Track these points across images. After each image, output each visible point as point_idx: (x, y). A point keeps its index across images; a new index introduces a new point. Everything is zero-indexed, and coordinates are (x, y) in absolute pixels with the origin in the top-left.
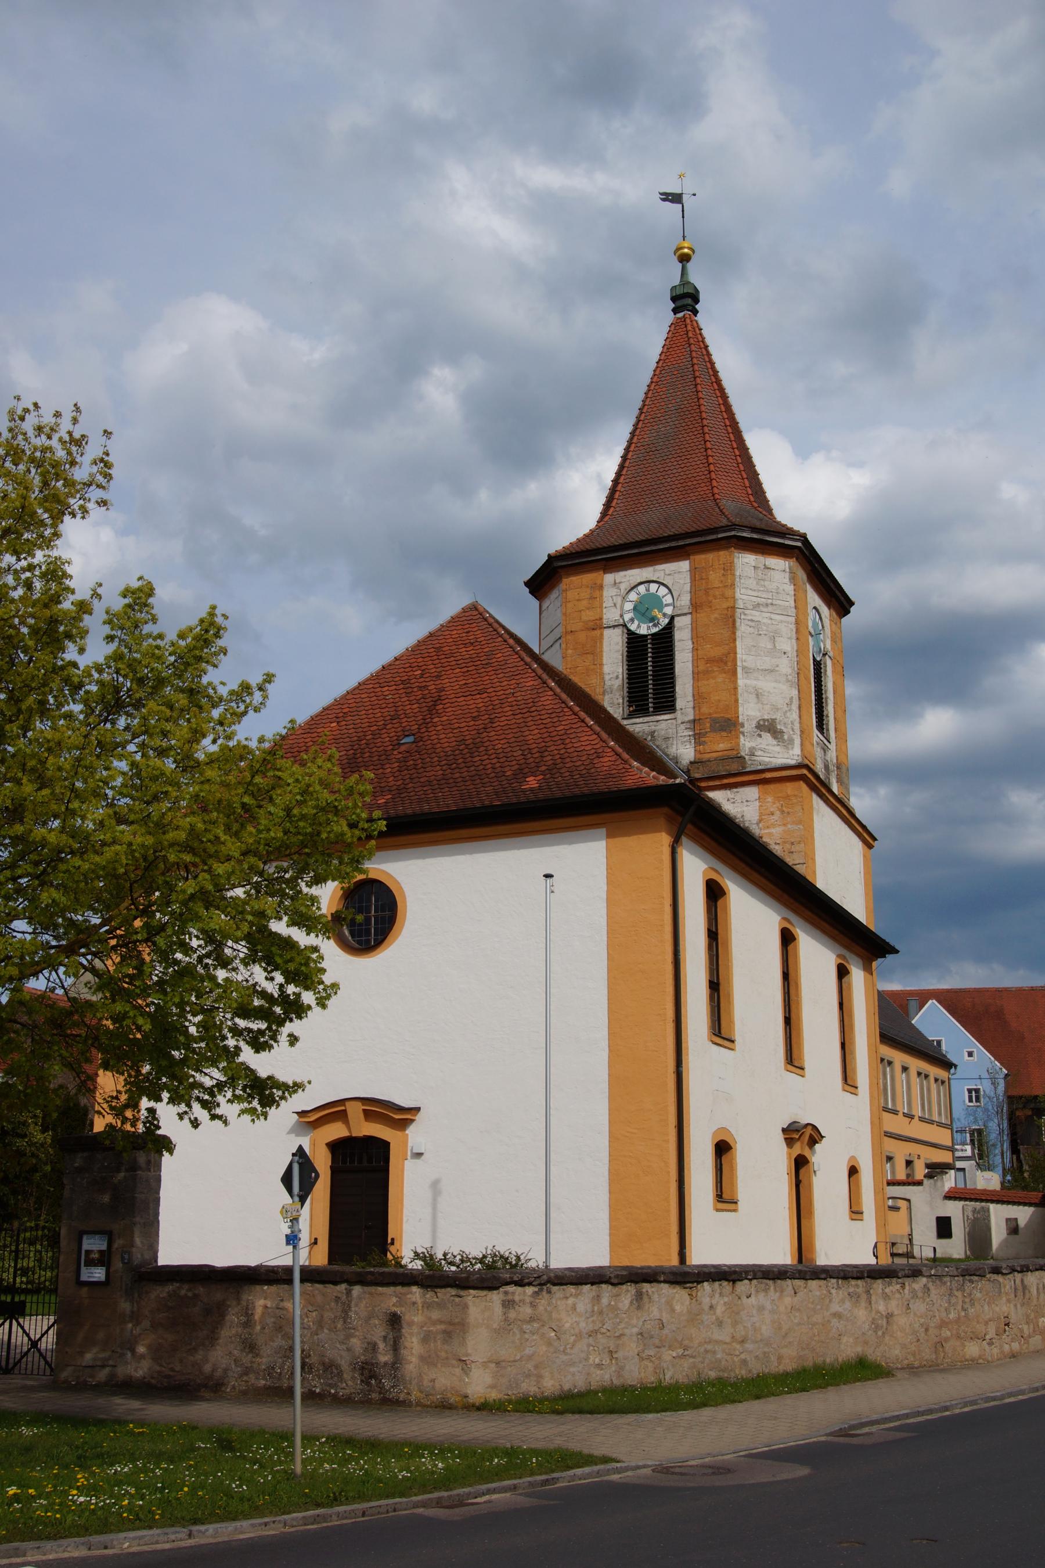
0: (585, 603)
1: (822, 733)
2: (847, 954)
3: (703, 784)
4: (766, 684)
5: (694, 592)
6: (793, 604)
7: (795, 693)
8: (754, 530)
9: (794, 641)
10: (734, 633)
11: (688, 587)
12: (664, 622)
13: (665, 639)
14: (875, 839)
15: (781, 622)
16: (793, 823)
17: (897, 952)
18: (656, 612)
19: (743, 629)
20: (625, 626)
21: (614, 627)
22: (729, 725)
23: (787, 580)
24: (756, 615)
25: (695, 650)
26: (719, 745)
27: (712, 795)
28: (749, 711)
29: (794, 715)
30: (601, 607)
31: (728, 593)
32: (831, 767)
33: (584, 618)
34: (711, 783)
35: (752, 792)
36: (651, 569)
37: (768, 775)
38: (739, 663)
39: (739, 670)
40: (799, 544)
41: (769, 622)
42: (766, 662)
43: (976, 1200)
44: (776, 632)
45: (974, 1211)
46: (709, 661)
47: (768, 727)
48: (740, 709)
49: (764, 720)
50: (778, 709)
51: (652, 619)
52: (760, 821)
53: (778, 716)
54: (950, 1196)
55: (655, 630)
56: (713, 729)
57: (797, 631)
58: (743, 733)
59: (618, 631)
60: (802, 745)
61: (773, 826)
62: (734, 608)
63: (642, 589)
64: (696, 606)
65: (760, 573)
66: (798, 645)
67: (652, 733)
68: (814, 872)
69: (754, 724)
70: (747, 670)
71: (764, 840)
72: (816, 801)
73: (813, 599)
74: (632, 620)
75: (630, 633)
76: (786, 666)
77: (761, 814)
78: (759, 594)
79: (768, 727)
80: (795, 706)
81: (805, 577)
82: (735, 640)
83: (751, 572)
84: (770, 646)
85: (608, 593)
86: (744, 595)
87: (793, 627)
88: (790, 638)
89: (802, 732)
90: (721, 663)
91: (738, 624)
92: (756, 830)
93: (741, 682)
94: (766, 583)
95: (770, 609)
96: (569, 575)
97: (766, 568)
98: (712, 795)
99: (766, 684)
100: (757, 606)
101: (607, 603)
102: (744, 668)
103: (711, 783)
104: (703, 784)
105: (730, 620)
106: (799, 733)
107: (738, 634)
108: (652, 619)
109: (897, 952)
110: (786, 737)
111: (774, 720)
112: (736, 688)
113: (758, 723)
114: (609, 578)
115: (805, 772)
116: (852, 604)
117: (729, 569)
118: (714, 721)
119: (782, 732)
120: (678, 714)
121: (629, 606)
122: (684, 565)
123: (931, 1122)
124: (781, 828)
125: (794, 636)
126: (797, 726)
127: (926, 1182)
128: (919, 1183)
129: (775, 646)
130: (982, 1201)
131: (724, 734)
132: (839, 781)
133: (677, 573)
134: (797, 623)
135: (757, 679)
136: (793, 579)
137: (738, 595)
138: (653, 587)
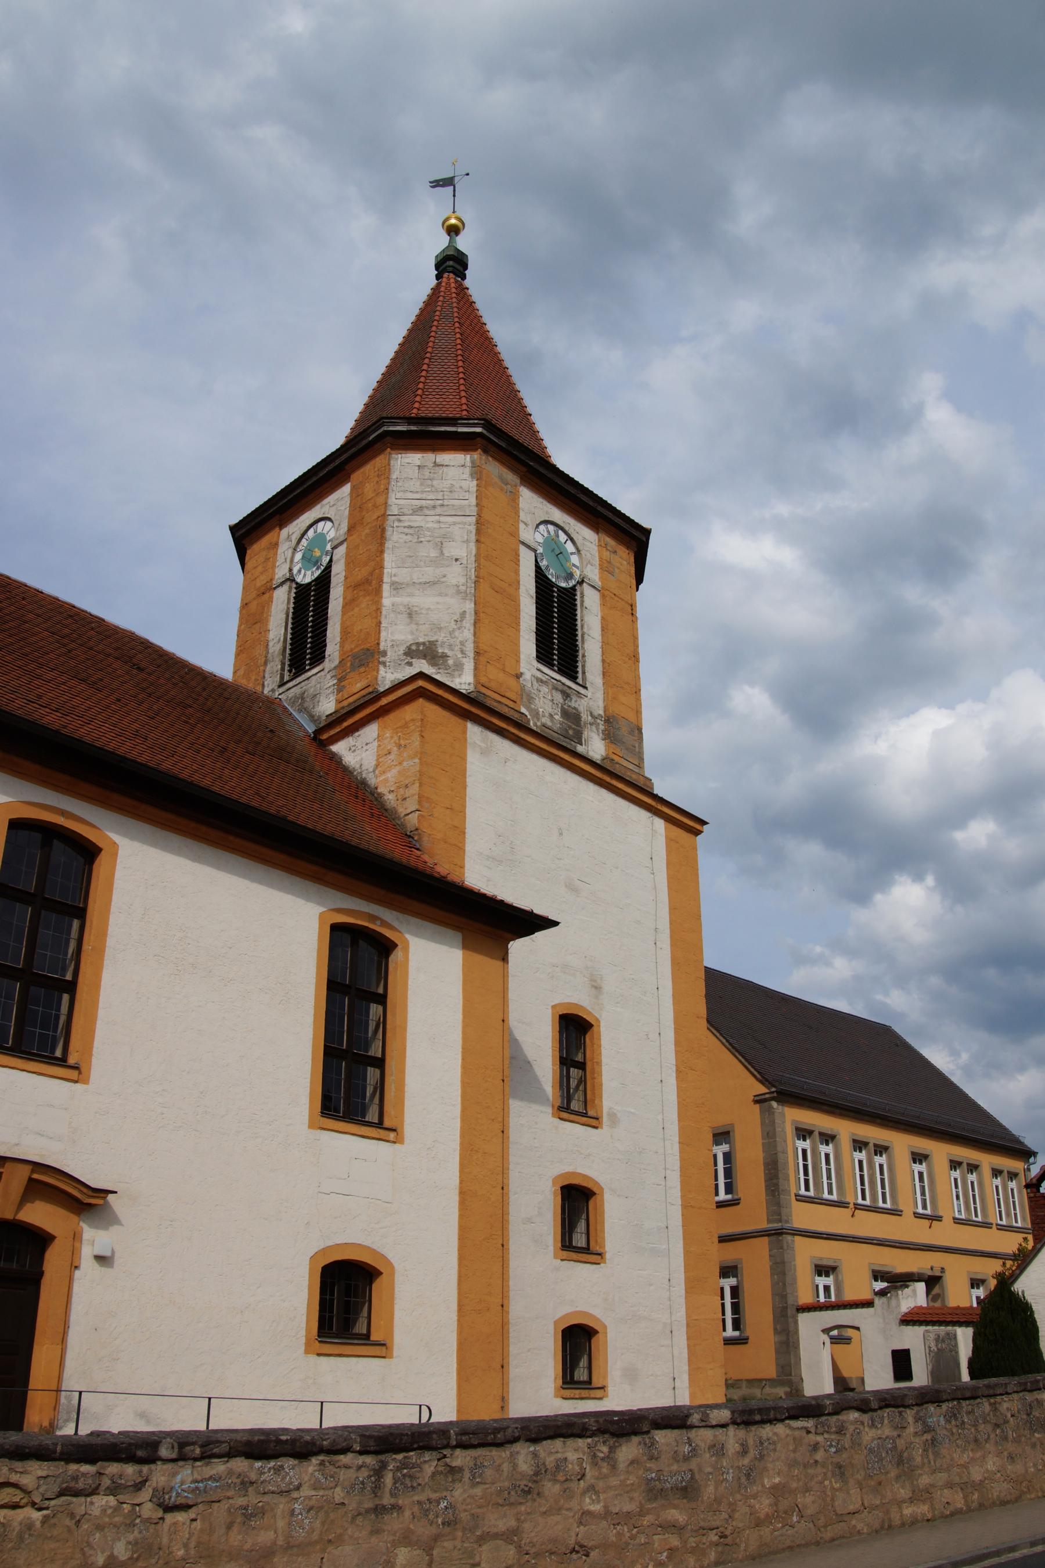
0: (260, 569)
1: (573, 678)
2: (388, 915)
3: (325, 736)
4: (423, 600)
5: (351, 515)
6: (473, 501)
7: (469, 606)
8: (410, 420)
9: (473, 546)
11: (347, 512)
12: (325, 560)
13: (323, 582)
14: (703, 823)
15: (455, 524)
16: (411, 758)
17: (555, 924)
18: (317, 553)
19: (395, 537)
20: (291, 579)
21: (282, 584)
22: (367, 655)
24: (417, 520)
25: (346, 578)
26: (357, 685)
27: (335, 748)
28: (395, 635)
29: (467, 633)
30: (274, 567)
31: (380, 500)
32: (585, 717)
33: (259, 584)
34: (332, 732)
35: (371, 731)
36: (318, 507)
37: (384, 701)
38: (386, 579)
39: (386, 587)
40: (479, 430)
41: (436, 525)
42: (430, 573)
43: (940, 1323)
44: (444, 536)
45: (938, 1339)
46: (357, 586)
48: (383, 634)
49: (418, 644)
50: (440, 629)
51: (317, 563)
52: (377, 766)
53: (440, 637)
54: (909, 1320)
55: (317, 573)
56: (353, 668)
57: (478, 532)
58: (384, 664)
59: (286, 587)
60: (476, 669)
61: (390, 768)
62: (384, 516)
63: (311, 533)
64: (351, 529)
65: (426, 472)
66: (478, 549)
67: (302, 697)
68: (460, 831)
69: (402, 649)
70: (396, 587)
71: (379, 790)
72: (474, 732)
73: (532, 504)
74: (299, 571)
75: (299, 586)
76: (458, 576)
77: (379, 757)
78: (424, 496)
79: (428, 651)
80: (468, 623)
81: (511, 477)
82: (382, 552)
83: (414, 473)
84: (434, 553)
85: (284, 549)
86: (397, 500)
87: (473, 528)
88: (467, 541)
89: (477, 653)
90: (368, 585)
91: (389, 531)
92: (372, 781)
93: (387, 601)
94: (435, 483)
95: (439, 511)
96: (252, 543)
97: (436, 464)
98: (335, 748)
99: (423, 600)
100: (418, 510)
101: (280, 558)
102: (393, 583)
103: (332, 732)
104: (325, 736)
105: (380, 536)
106: (472, 655)
107: (388, 545)
108: (317, 563)
109: (555, 924)
110: (450, 662)
111: (433, 644)
112: (378, 610)
113: (409, 648)
114: (284, 532)
115: (421, 683)
116: (647, 532)
117: (385, 474)
118: (355, 657)
119: (445, 656)
120: (328, 664)
121: (298, 556)
122: (346, 489)
123: (986, 1225)
124: (398, 768)
125: (473, 537)
126: (470, 648)
127: (877, 1301)
128: (869, 1304)
129: (442, 553)
130: (947, 1323)
131: (362, 669)
132: (610, 736)
133: (338, 502)
134: (480, 524)
135: (411, 595)
136: (477, 473)
137: (392, 500)
138: (321, 524)
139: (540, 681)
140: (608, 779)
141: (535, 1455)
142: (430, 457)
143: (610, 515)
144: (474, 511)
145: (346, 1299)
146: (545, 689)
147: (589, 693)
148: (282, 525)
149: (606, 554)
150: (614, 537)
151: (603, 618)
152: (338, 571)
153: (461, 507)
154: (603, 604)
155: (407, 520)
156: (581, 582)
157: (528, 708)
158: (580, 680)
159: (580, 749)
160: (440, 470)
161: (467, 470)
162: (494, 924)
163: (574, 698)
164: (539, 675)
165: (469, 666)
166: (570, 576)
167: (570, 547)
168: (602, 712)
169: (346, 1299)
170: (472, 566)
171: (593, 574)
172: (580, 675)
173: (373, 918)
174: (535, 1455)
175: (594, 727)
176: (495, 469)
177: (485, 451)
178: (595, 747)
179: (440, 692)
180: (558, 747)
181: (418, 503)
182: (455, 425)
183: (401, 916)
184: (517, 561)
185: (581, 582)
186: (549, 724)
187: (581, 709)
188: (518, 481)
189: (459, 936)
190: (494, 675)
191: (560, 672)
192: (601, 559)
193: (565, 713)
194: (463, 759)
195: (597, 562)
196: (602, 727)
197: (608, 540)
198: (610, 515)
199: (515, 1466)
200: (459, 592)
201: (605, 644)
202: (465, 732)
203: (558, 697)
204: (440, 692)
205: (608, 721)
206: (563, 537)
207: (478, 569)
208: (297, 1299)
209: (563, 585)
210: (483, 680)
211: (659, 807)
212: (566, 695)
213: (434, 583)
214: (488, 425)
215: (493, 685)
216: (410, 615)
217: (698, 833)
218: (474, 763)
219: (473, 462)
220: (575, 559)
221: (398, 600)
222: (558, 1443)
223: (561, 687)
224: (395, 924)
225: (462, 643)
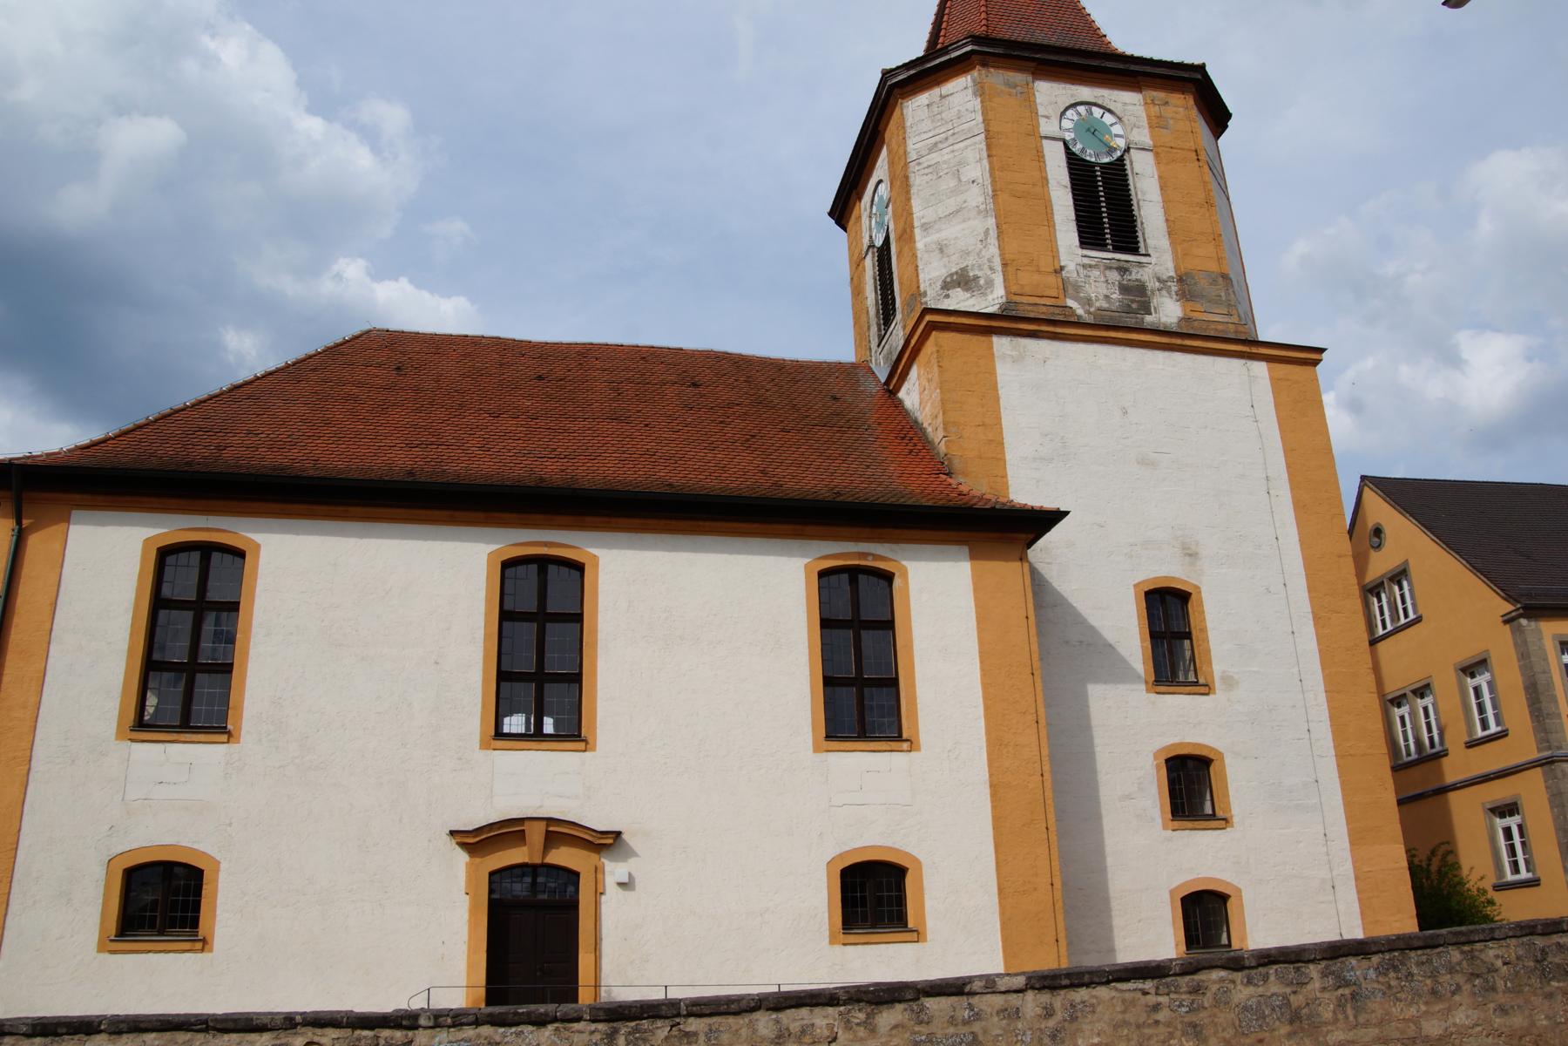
4: (950, 232)
7: (991, 222)
9: (985, 163)
10: (908, 192)
14: (1322, 350)
23: (970, 97)
24: (935, 157)
29: (993, 250)
32: (1152, 284)
38: (916, 224)
39: (917, 231)
42: (952, 203)
44: (960, 163)
47: (962, 280)
48: (921, 276)
53: (970, 261)
57: (989, 147)
65: (935, 109)
69: (939, 284)
70: (926, 227)
76: (976, 197)
81: (1018, 77)
82: (909, 199)
84: (953, 183)
87: (983, 146)
89: (1005, 265)
90: (907, 235)
91: (912, 176)
95: (951, 141)
97: (942, 97)
99: (950, 232)
100: (933, 148)
107: (913, 191)
109: (1067, 513)
110: (982, 282)
111: (964, 270)
112: (915, 256)
115: (928, 318)
119: (976, 278)
125: (985, 154)
126: (997, 263)
135: (939, 231)
139: (1084, 266)
140: (1179, 341)
141: (777, 1021)
142: (936, 92)
143: (1149, 69)
144: (981, 128)
145: (873, 894)
146: (1096, 273)
147: (1153, 260)
148: (860, 199)
149: (1155, 110)
150: (1163, 88)
151: (1160, 177)
152: (892, 227)
153: (970, 129)
154: (1158, 162)
155: (925, 161)
156: (1127, 150)
157: (1075, 299)
158: (1142, 250)
159: (1149, 319)
160: (945, 101)
161: (970, 91)
162: (1012, 529)
163: (1134, 271)
164: (1086, 261)
165: (998, 279)
166: (1111, 150)
167: (1108, 119)
168: (1172, 274)
169: (873, 894)
170: (988, 182)
171: (1143, 136)
172: (1142, 245)
173: (864, 555)
174: (777, 1021)
175: (1164, 292)
176: (998, 78)
177: (984, 65)
178: (1168, 311)
179: (952, 319)
180: (1123, 327)
181: (933, 140)
182: (947, 53)
183: (894, 546)
184: (1040, 157)
185: (1127, 150)
186: (1105, 305)
187: (1145, 278)
188: (1030, 78)
189: (966, 549)
190: (1027, 279)
191: (1117, 249)
192: (1149, 117)
193: (1124, 289)
194: (993, 373)
195: (1144, 122)
196: (1174, 289)
197: (1155, 94)
198: (1149, 69)
199: (755, 1031)
200: (980, 212)
201: (1167, 201)
202: (991, 347)
203: (1114, 276)
204: (952, 319)
205: (1180, 280)
206: (1097, 112)
207: (994, 182)
208: (818, 899)
209: (1106, 160)
210: (1014, 289)
211: (1254, 350)
212: (1123, 270)
213: (957, 212)
214: (975, 39)
215: (1027, 290)
216: (941, 250)
217: (1316, 363)
218: (1005, 373)
219: (974, 80)
220: (1117, 129)
221: (928, 239)
222: (804, 1011)
223: (1115, 264)
224: (889, 555)
225: (989, 260)
